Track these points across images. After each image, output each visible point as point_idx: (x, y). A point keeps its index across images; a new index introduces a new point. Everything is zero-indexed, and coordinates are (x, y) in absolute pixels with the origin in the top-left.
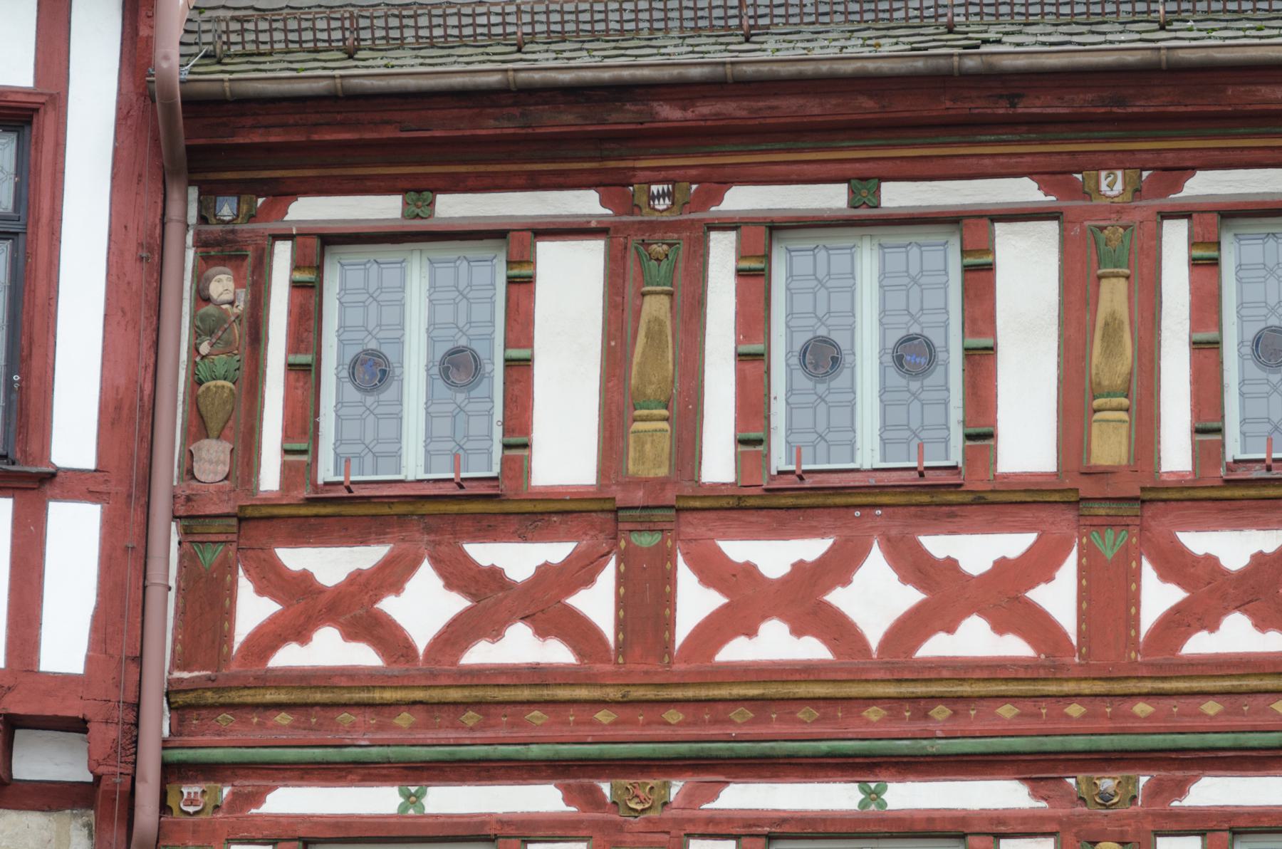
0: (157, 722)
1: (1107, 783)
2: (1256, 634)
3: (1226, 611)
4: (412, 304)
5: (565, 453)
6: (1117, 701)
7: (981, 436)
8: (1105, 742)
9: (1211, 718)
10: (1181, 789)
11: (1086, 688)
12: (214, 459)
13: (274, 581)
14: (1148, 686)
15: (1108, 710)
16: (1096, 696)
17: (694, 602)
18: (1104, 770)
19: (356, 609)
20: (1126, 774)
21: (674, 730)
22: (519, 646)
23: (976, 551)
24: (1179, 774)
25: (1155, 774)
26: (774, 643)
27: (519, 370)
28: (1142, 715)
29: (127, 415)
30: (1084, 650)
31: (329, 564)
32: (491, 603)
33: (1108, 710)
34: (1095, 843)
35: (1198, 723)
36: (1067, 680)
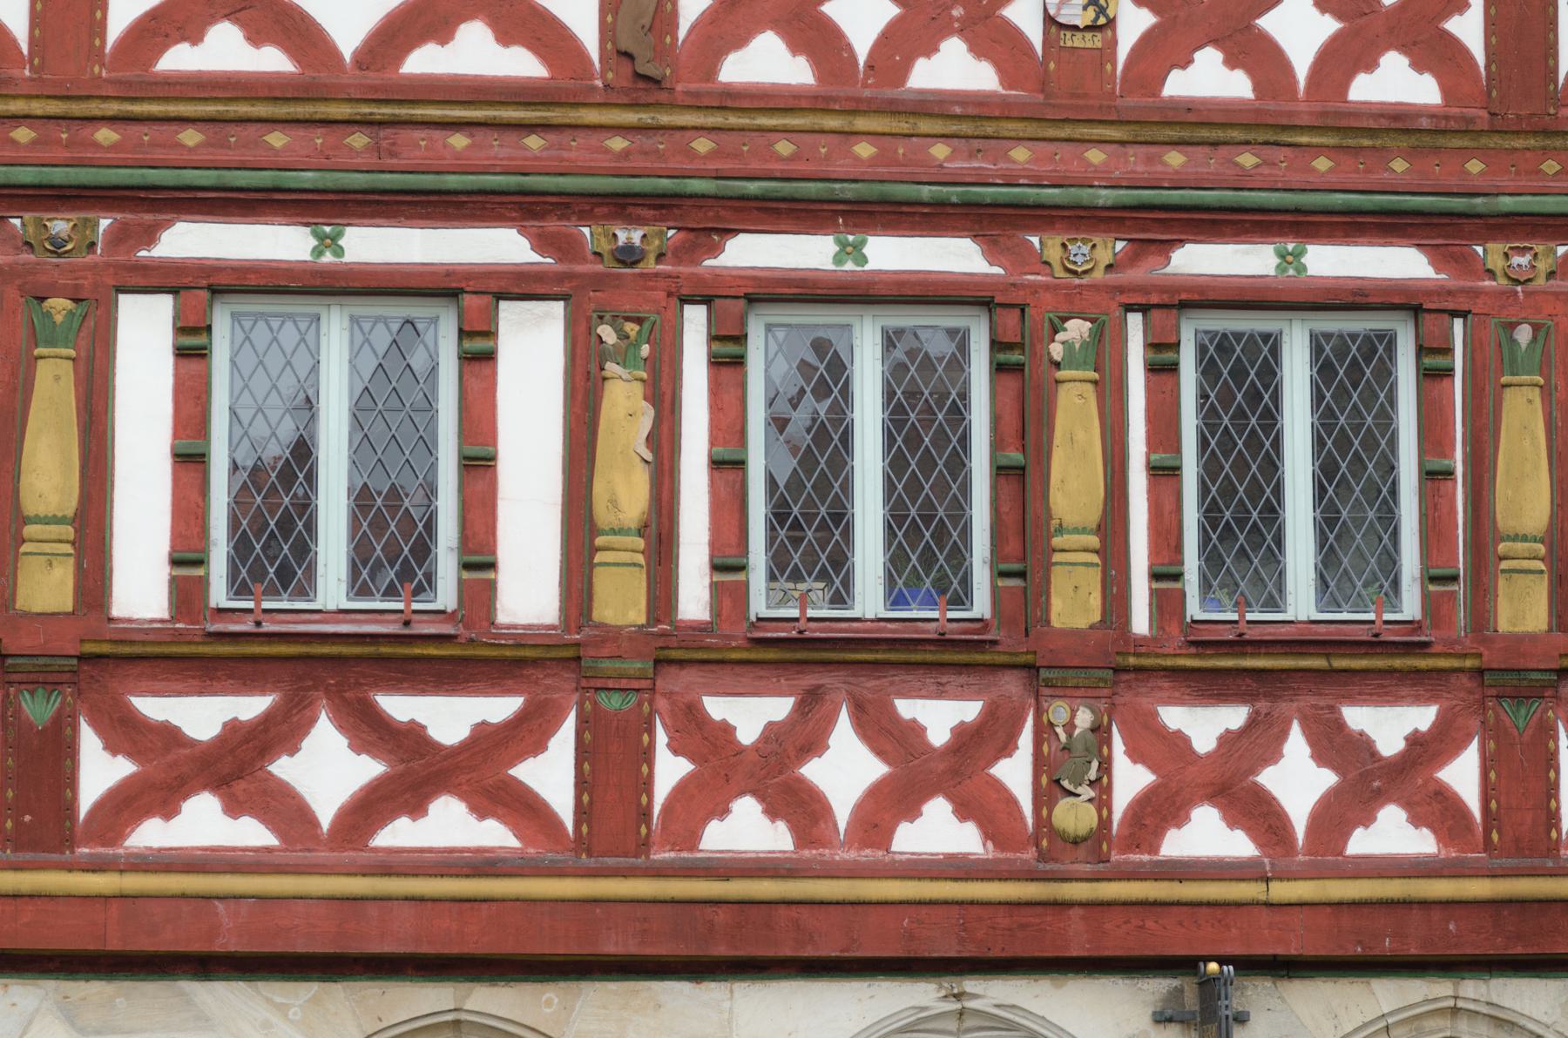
1: (60, 226)
2: (249, 49)
3: (213, 20)
6: (75, 125)
8: (58, 175)
9: (190, 150)
10: (150, 236)
11: (37, 107)
14: (113, 108)
15: (64, 136)
16: (49, 118)
18: (57, 210)
20: (83, 215)
24: (148, 217)
25: (119, 216)
28: (106, 143)
30: (36, 61)
33: (64, 136)
34: (42, 299)
35: (173, 156)
36: (15, 97)
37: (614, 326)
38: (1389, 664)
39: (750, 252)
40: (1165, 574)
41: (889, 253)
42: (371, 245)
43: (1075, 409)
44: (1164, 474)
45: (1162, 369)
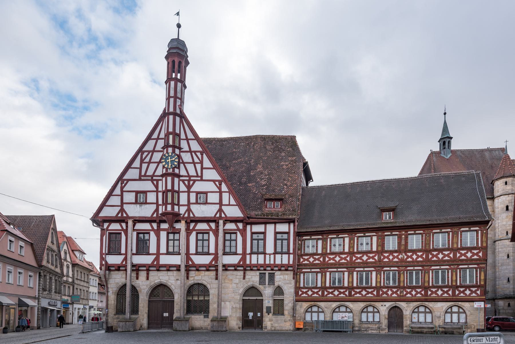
0: (296, 266)
4: (310, 243)
5: (320, 251)
7: (344, 250)
12: (299, 252)
13: (303, 258)
17: (327, 259)
19: (307, 260)
21: (326, 266)
22: (317, 262)
23: (343, 256)
26: (332, 261)
27: (317, 247)
29: (294, 250)
31: (306, 257)
32: (315, 259)
37: (378, 272)
38: (419, 287)
39: (385, 269)
40: (407, 283)
41: (392, 269)
42: (366, 269)
43: (402, 275)
44: (407, 278)
45: (407, 273)
